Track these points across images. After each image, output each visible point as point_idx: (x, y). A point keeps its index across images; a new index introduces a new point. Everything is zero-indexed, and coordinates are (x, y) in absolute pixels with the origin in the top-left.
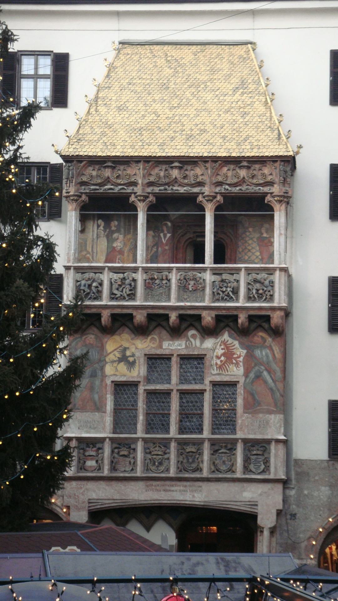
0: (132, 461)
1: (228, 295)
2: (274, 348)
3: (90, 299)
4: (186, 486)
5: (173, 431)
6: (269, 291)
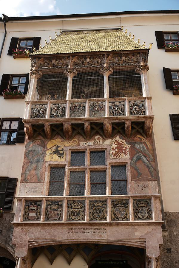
0: (59, 213)
1: (119, 112)
2: (147, 143)
3: (38, 118)
4: (95, 229)
5: (86, 194)
6: (143, 109)
